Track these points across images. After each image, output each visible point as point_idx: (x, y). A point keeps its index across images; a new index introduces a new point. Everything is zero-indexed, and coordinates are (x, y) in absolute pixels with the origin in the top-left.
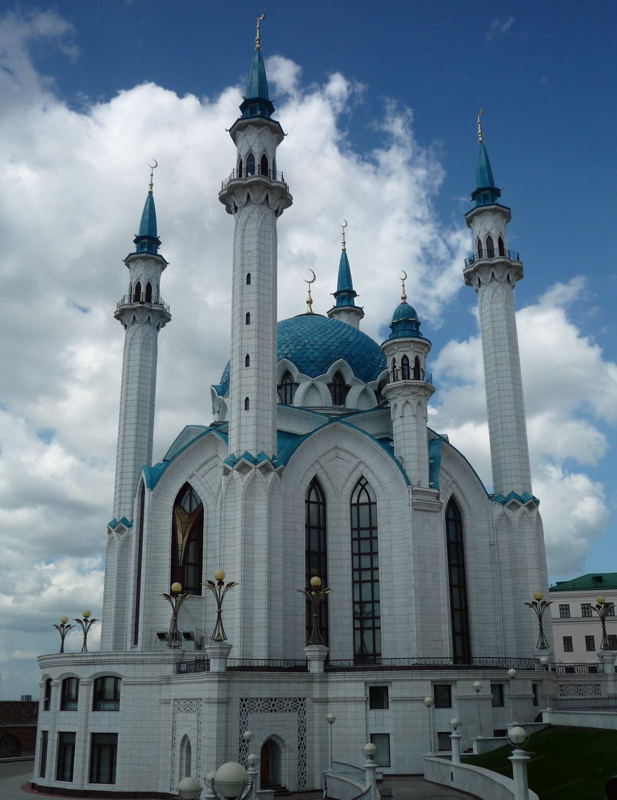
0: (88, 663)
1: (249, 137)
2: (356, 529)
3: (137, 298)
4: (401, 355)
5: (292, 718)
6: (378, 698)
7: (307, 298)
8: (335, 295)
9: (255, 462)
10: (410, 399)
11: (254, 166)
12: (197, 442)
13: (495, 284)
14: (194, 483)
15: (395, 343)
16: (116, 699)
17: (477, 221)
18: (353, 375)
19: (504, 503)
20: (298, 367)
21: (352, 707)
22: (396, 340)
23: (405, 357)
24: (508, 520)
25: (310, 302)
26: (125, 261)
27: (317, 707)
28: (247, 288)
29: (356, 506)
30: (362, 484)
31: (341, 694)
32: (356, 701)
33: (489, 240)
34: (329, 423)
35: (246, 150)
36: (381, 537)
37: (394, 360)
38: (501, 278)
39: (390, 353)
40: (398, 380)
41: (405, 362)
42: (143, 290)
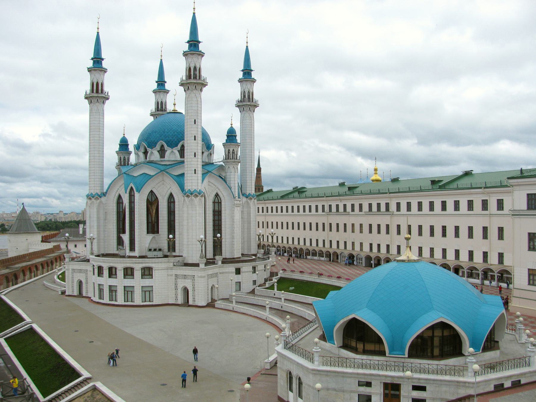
0: (139, 263)
2: (214, 211)
5: (215, 279)
6: (238, 271)
7: (173, 103)
8: (157, 82)
9: (199, 194)
13: (249, 112)
14: (155, 191)
16: (151, 275)
17: (245, 83)
19: (247, 197)
21: (231, 275)
24: (248, 203)
25: (175, 105)
27: (222, 275)
29: (214, 202)
30: (217, 195)
31: (227, 271)
32: (232, 273)
36: (223, 215)
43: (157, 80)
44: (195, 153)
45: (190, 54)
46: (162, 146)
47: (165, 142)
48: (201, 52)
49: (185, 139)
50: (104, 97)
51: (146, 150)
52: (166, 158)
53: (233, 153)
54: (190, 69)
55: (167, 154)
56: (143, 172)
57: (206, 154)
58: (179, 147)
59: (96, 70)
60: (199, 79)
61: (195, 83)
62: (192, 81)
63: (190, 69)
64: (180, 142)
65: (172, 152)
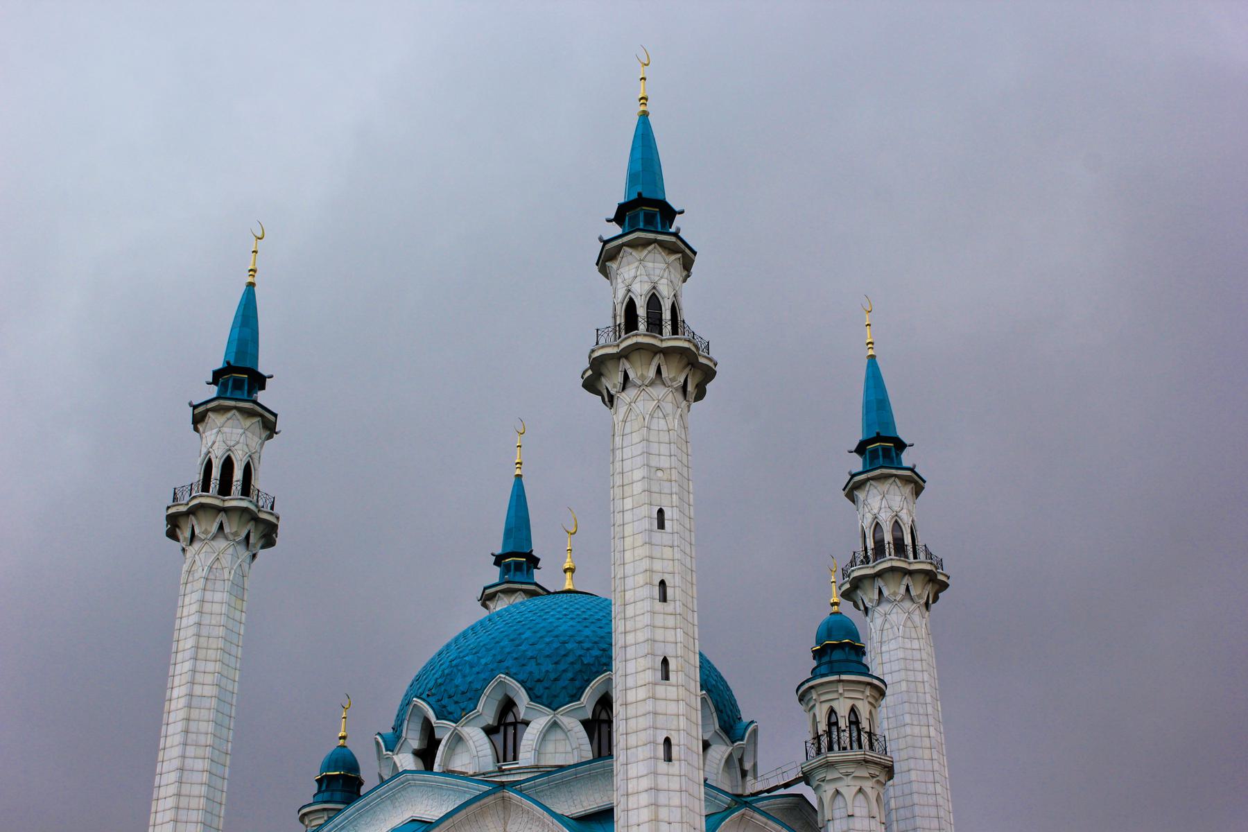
1: (650, 265)
3: (206, 487)
4: (849, 703)
10: (868, 785)
11: (661, 320)
12: (474, 806)
13: (907, 605)
15: (840, 681)
18: (717, 726)
20: (529, 691)
22: (844, 677)
23: (853, 710)
26: (195, 407)
28: (658, 536)
33: (897, 525)
34: (729, 810)
35: (647, 287)
37: (832, 711)
38: (919, 596)
39: (823, 698)
40: (845, 749)
41: (853, 719)
42: (238, 474)
43: (499, 551)
44: (665, 662)
45: (631, 245)
46: (508, 705)
47: (522, 683)
48: (676, 235)
49: (617, 664)
50: (255, 519)
51: (428, 731)
52: (526, 756)
53: (855, 722)
54: (631, 307)
55: (530, 737)
56: (407, 815)
57: (720, 751)
58: (588, 699)
59: (227, 409)
60: (675, 331)
61: (654, 351)
62: (640, 340)
63: (631, 307)
64: (589, 681)
65: (554, 725)
